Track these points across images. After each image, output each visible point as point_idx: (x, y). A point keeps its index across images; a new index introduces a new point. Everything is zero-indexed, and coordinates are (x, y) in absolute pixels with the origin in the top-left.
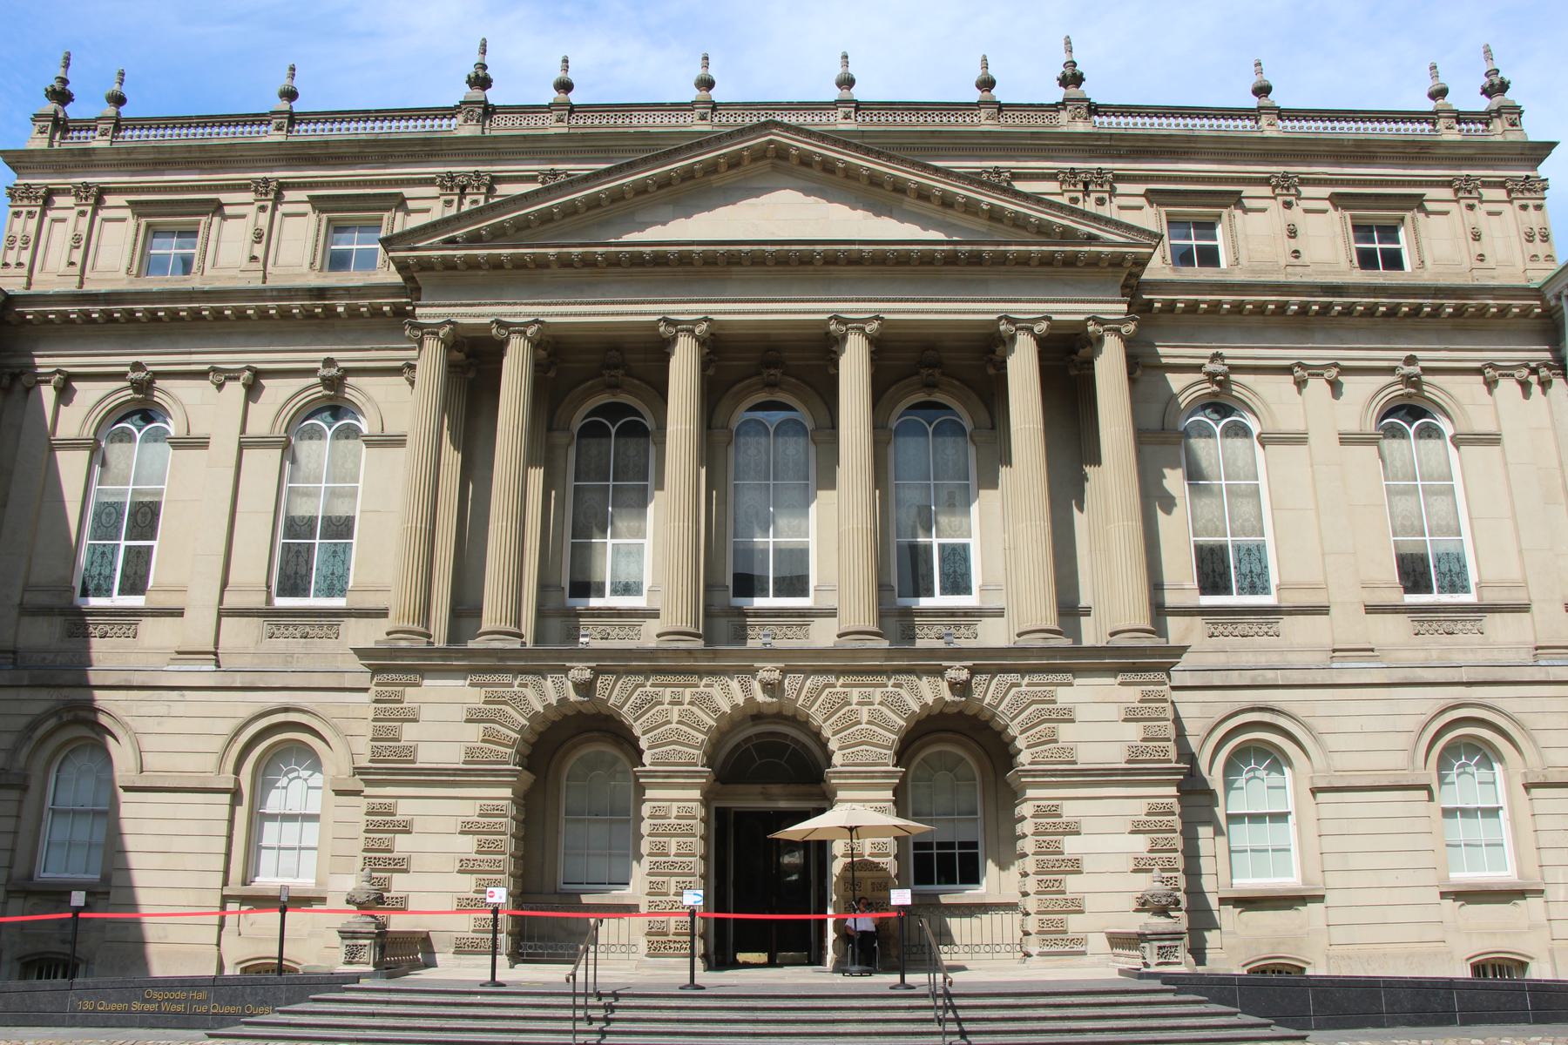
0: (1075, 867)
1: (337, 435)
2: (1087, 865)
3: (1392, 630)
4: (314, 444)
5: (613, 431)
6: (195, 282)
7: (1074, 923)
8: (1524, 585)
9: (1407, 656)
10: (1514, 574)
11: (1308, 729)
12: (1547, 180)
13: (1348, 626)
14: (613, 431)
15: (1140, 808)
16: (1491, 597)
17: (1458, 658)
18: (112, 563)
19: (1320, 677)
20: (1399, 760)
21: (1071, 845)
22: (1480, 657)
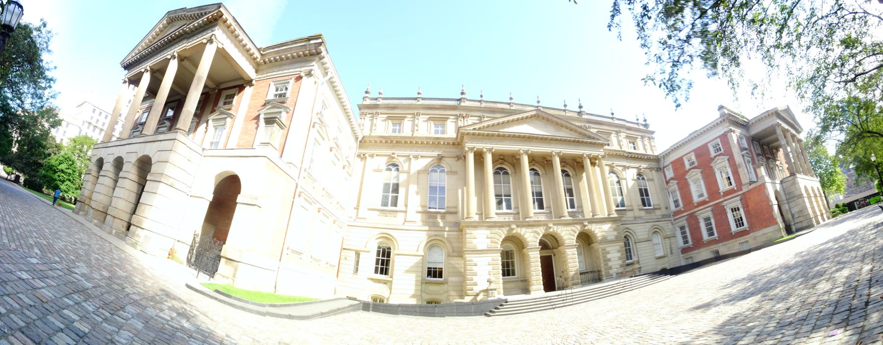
0: (609, 260)
1: (440, 172)
2: (612, 260)
3: (643, 213)
4: (436, 173)
5: (501, 173)
6: (402, 135)
7: (611, 272)
8: (659, 205)
9: (647, 218)
10: (658, 203)
11: (634, 232)
12: (653, 132)
13: (637, 213)
14: (501, 173)
15: (618, 248)
16: (656, 207)
17: (652, 217)
18: (388, 199)
19: (634, 222)
20: (646, 236)
21: (609, 256)
22: (655, 217)
